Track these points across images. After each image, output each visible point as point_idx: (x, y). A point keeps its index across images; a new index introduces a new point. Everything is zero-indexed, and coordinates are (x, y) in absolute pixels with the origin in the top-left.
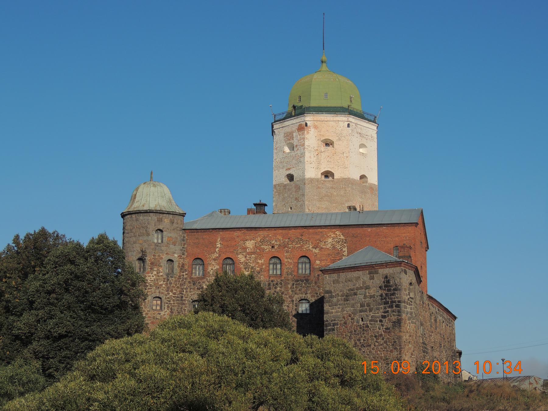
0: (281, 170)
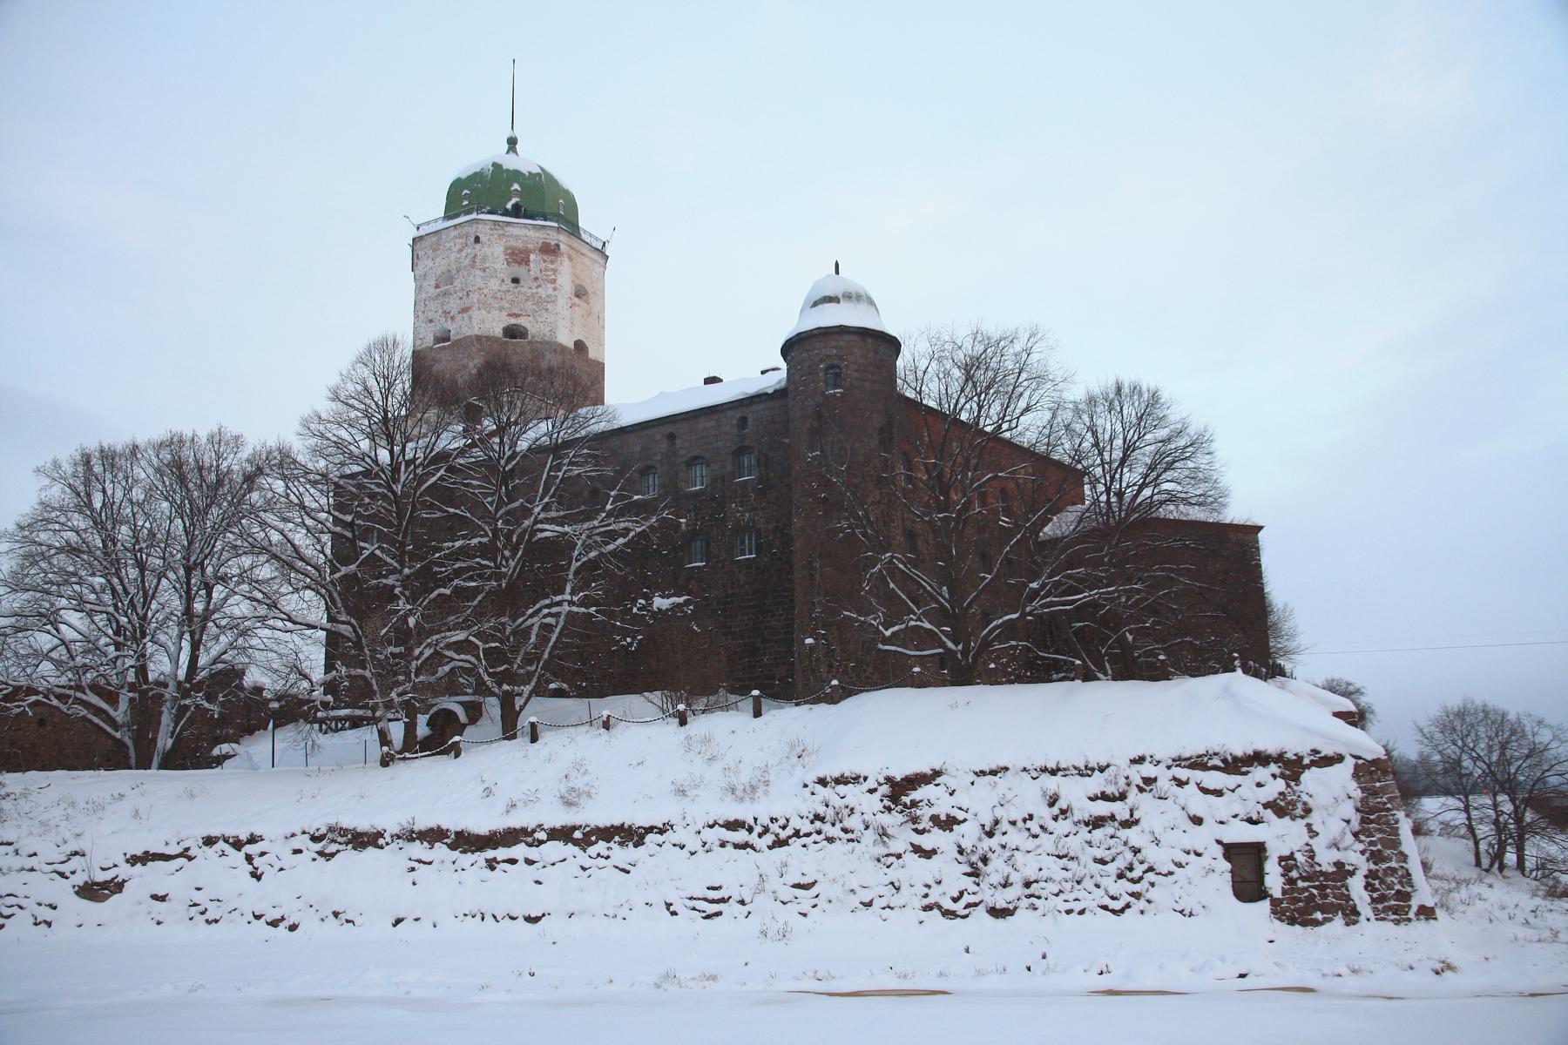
0: (495, 312)
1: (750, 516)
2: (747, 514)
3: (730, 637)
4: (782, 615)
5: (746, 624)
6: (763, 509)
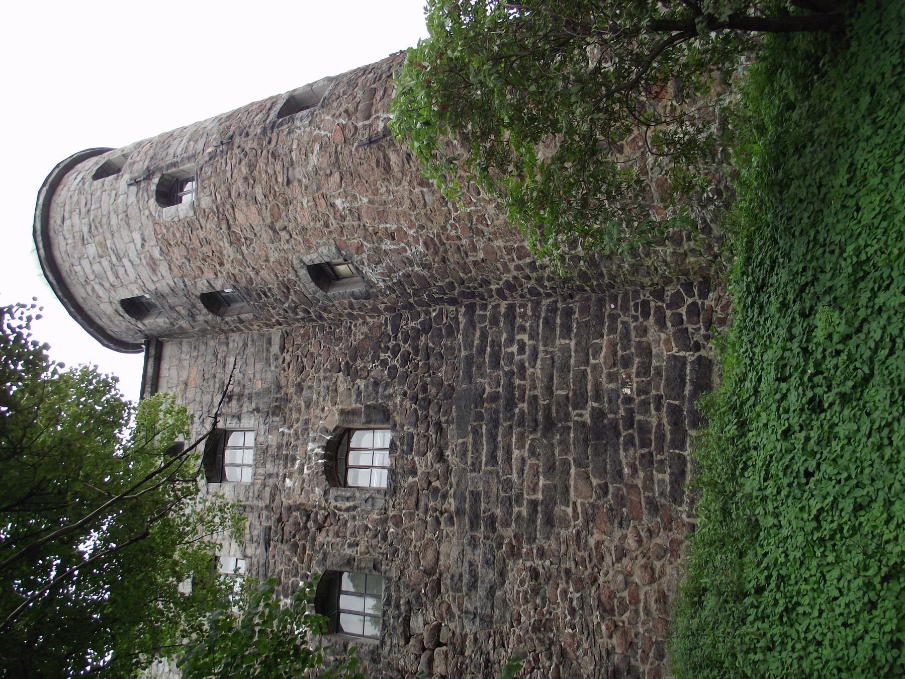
1: (314, 440)
2: (310, 446)
3: (559, 509)
4: (522, 350)
5: (532, 453)
6: (308, 407)
